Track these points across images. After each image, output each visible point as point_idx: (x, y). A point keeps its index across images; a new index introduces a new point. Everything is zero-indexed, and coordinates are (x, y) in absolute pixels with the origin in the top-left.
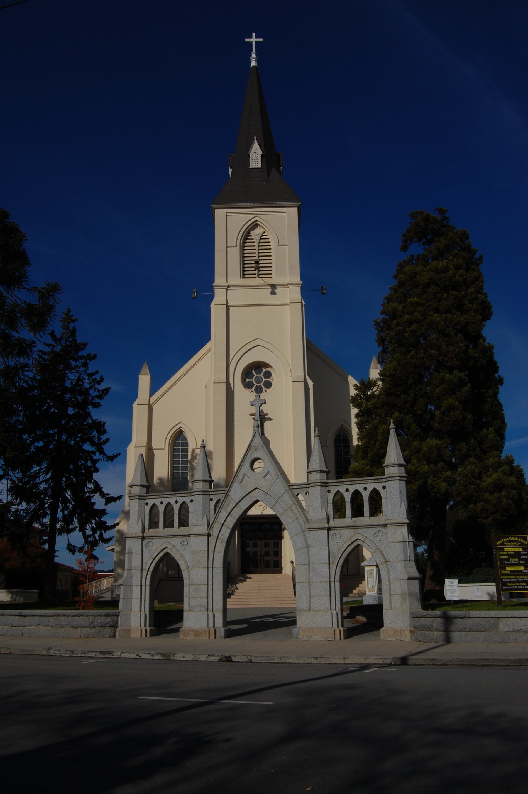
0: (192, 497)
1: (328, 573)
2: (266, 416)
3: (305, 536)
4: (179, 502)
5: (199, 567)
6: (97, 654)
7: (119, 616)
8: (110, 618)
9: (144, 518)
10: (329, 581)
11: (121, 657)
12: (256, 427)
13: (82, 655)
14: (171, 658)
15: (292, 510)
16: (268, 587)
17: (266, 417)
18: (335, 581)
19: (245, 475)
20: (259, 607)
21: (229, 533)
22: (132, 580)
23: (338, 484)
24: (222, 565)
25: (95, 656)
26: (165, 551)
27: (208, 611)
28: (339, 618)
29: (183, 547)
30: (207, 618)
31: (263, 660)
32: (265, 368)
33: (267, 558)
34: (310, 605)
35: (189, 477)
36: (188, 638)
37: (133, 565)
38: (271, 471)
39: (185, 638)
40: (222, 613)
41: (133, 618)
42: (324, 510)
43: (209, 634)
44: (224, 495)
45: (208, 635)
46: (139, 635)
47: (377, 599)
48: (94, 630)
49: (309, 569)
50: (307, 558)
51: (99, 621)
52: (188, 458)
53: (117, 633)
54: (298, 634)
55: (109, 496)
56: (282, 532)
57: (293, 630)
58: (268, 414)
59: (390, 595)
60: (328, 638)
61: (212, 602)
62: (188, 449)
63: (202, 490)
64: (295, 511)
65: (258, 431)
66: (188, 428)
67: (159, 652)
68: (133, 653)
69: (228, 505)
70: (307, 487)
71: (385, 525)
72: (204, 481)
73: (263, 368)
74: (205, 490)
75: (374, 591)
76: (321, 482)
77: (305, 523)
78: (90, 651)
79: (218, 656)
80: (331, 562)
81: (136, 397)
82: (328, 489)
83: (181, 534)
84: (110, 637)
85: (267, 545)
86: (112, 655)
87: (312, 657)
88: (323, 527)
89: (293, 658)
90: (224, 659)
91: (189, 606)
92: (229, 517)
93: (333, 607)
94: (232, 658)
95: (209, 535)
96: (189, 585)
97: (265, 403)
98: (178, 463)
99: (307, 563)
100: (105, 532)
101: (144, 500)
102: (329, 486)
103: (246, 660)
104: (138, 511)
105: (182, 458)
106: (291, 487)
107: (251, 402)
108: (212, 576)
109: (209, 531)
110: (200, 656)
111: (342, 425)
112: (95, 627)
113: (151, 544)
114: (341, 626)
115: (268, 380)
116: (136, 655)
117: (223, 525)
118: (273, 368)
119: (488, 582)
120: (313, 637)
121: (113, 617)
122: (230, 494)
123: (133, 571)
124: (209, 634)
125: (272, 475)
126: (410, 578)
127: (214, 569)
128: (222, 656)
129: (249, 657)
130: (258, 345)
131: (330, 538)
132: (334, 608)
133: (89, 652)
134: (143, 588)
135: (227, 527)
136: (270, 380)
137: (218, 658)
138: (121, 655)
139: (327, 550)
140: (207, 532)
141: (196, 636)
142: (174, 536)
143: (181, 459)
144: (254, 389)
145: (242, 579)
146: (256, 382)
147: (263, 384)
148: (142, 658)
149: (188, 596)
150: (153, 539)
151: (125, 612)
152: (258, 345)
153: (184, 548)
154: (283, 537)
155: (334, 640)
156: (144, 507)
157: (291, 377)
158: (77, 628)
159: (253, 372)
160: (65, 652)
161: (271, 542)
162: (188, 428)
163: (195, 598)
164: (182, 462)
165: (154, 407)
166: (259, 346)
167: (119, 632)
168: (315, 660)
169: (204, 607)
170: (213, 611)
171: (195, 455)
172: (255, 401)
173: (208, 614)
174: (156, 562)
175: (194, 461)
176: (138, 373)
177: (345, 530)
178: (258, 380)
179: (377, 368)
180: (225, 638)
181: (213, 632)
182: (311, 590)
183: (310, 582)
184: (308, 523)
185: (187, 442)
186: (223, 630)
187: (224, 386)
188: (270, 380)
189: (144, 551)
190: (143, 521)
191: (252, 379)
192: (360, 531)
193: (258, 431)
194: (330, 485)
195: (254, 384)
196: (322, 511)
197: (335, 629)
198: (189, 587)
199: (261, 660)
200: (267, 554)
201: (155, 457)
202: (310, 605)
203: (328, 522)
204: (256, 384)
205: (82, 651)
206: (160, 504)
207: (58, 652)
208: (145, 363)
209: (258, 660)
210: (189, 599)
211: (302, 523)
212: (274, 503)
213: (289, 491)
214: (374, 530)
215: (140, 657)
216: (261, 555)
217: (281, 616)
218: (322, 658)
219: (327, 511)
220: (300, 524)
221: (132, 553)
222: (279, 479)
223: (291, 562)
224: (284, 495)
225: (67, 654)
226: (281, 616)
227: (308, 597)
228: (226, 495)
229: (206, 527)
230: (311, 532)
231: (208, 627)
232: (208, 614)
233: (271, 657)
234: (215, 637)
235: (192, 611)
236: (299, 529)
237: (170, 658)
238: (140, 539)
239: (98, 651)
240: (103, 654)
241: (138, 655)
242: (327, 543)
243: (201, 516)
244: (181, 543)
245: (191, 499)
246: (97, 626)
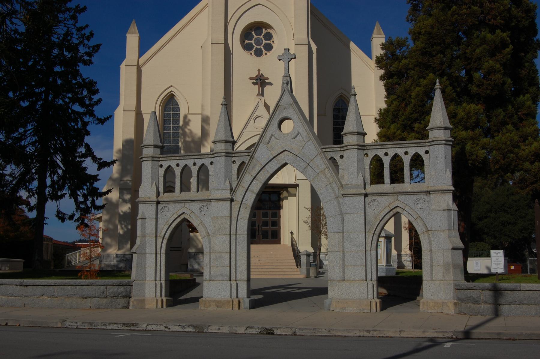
0: (213, 159)
1: (364, 242)
2: (266, 80)
3: (338, 202)
4: (197, 165)
5: (220, 234)
6: (119, 326)
7: (132, 286)
8: (123, 288)
9: (158, 181)
10: (365, 250)
11: (147, 329)
12: (285, 84)
13: (102, 328)
14: (205, 330)
15: (325, 174)
16: (268, 258)
17: (267, 81)
18: (371, 251)
19: (272, 136)
20: (261, 277)
21: (254, 198)
22: (146, 247)
23: (376, 148)
24: (246, 233)
25: (117, 328)
26: (182, 217)
27: (230, 280)
28: (375, 289)
29: (203, 213)
30: (230, 288)
31: (309, 333)
32: (266, 30)
33: (264, 229)
34: (343, 275)
35: (180, 144)
36: (209, 309)
37: (147, 232)
38: (301, 132)
39: (205, 309)
40: (246, 282)
41: (147, 288)
42: (360, 175)
43: (233, 304)
44: (249, 157)
45: (231, 305)
46: (155, 306)
47: (385, 271)
48: (105, 300)
49: (343, 237)
50: (341, 225)
51: (111, 291)
52: (179, 124)
53: (131, 304)
54: (330, 305)
55: (102, 161)
56: (281, 202)
57: (324, 301)
58: (269, 79)
59: (432, 266)
60: (363, 309)
61: (235, 271)
62: (179, 115)
63: (224, 151)
64: (329, 175)
65: (287, 88)
66: (180, 92)
67: (191, 324)
68: (161, 325)
69: (253, 168)
70: (342, 150)
71: (428, 192)
72: (227, 142)
73: (264, 30)
74: (227, 151)
75: (382, 262)
76: (358, 145)
77: (339, 188)
78: (112, 323)
79: (259, 328)
80: (367, 230)
81: (123, 57)
82: (365, 153)
83: (200, 198)
84: (123, 308)
85: (265, 215)
86: (137, 328)
87: (364, 330)
88: (359, 193)
89: (343, 331)
90: (265, 331)
91: (210, 275)
92: (254, 181)
93: (369, 277)
94: (274, 331)
95: (232, 200)
96: (210, 253)
97: (295, 58)
98: (169, 129)
99: (341, 231)
100: (97, 199)
101: (158, 162)
102: (367, 149)
103: (290, 333)
104: (152, 174)
105: (173, 123)
106: (324, 150)
107: (279, 56)
108: (235, 244)
109: (232, 195)
110: (237, 329)
111: (341, 93)
112: (106, 297)
113: (166, 209)
114: (376, 297)
115: (269, 42)
116: (165, 327)
117: (247, 189)
118: (274, 30)
119: (482, 257)
120: (347, 308)
121: (126, 286)
122: (255, 156)
123: (147, 238)
124: (233, 304)
125: (303, 136)
126: (454, 249)
127: (237, 236)
128: (262, 328)
129: (294, 330)
130: (259, 4)
131: (367, 205)
132: (370, 279)
133: (110, 324)
134: (158, 256)
135: (252, 192)
136: (271, 42)
137: (258, 330)
138: (147, 327)
139: (364, 218)
140: (229, 196)
141: (218, 307)
142: (193, 201)
144: (253, 52)
148: (171, 330)
149: (208, 265)
150: (169, 204)
151: (138, 281)
152: (259, 4)
153: (204, 213)
154: (282, 207)
155: (369, 312)
156: (158, 169)
157: (293, 39)
158: (86, 298)
159: (253, 33)
160: (83, 324)
161: (270, 212)
162: (180, 92)
163: (217, 267)
165: (143, 69)
166: (260, 5)
167: (133, 302)
168: (367, 332)
169: (226, 276)
170: (236, 281)
171: (187, 120)
172: (283, 55)
173: (231, 284)
174: (172, 228)
175: (186, 127)
176: (126, 32)
177: (383, 197)
178: (258, 42)
179: (380, 35)
180: (250, 309)
181: (237, 302)
182: (346, 260)
183: (343, 251)
184: (343, 188)
186: (247, 301)
187: (223, 46)
188: (271, 42)
189: (158, 217)
190: (157, 185)
192: (400, 197)
193: (287, 88)
194: (367, 148)
195: (254, 47)
196: (358, 176)
197: (371, 300)
198: (210, 255)
199: (307, 333)
200: (266, 224)
202: (343, 275)
203: (365, 188)
204: (256, 46)
205: (102, 323)
206: (176, 166)
207: (75, 325)
209: (303, 333)
210: (210, 268)
211: (336, 189)
212: (305, 167)
213: (322, 154)
214: (415, 197)
215: (169, 329)
216: (259, 225)
217: (291, 286)
218: (376, 331)
219: (363, 176)
220: (334, 190)
221: (146, 219)
222: (311, 141)
223: (290, 233)
224: (316, 159)
225: (85, 326)
226: (291, 286)
227: (341, 267)
228: (251, 157)
229: (229, 192)
230: (346, 199)
231: (231, 297)
232: (231, 284)
233: (318, 330)
234: (239, 309)
235: (214, 280)
236: (333, 195)
237: (204, 330)
239: (120, 323)
240: (127, 327)
241: (166, 327)
242: (363, 210)
243: (224, 179)
244: (201, 208)
245: (211, 161)
246: (108, 296)
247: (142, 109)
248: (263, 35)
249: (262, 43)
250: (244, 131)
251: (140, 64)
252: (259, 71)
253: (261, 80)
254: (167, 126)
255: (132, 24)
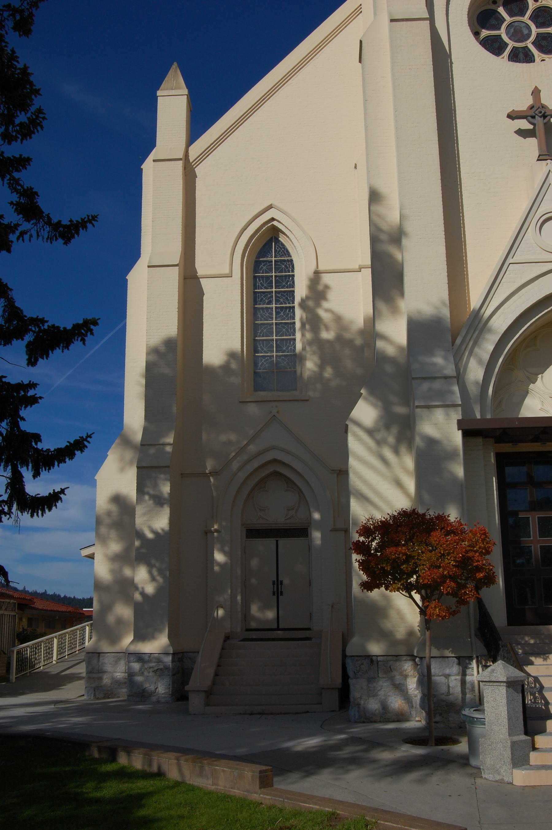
62: (293, 279)
66: (294, 220)
81: (152, 144)
100: (36, 474)
105: (277, 301)
143: (274, 306)
145: (532, 641)
146: (510, 38)
147: (533, 43)
159: (501, 10)
162: (294, 220)
164: (277, 313)
185: (292, 260)
191: (499, 29)
195: (506, 45)
201: (204, 298)
204: (511, 44)
208: (175, 64)
238: (193, 162)
247: (197, 265)
248: (529, 13)
249: (529, 35)
250: (510, 260)
251: (191, 159)
252: (536, 93)
253: (544, 116)
254: (262, 308)
255: (170, 72)
